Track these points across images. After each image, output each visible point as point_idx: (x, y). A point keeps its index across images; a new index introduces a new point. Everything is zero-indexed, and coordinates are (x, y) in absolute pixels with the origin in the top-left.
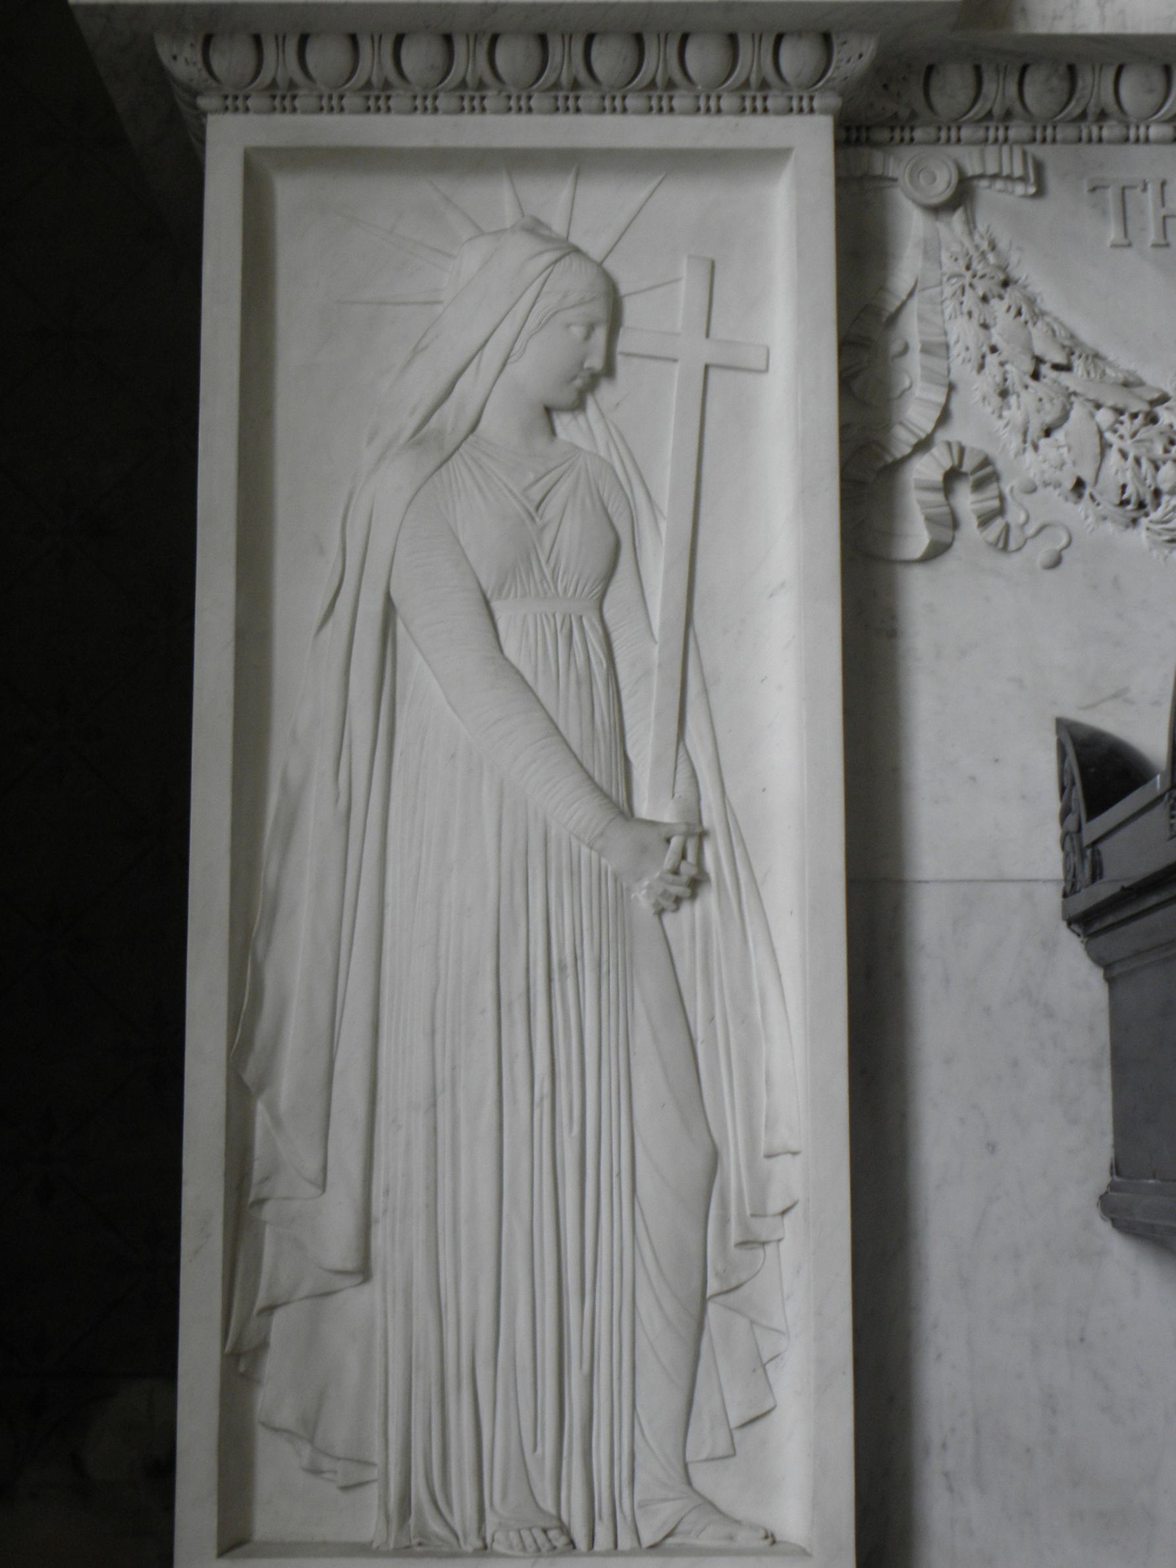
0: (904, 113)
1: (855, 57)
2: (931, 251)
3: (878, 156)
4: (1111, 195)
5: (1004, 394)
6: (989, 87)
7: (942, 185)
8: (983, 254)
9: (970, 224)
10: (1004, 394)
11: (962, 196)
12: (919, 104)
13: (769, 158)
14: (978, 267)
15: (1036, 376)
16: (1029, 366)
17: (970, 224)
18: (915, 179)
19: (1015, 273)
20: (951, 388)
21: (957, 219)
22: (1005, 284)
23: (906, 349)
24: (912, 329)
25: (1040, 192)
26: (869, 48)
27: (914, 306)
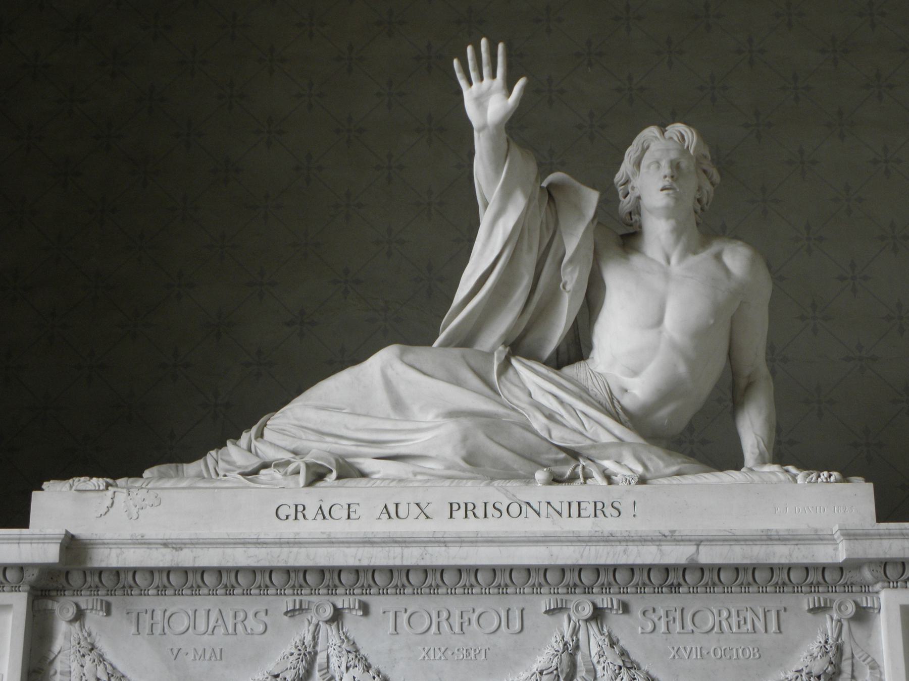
0: (60, 587)
1: (31, 576)
2: (67, 637)
3: (50, 603)
4: (134, 615)
6: (89, 579)
7: (71, 612)
8: (86, 638)
9: (82, 627)
11: (80, 616)
12: (65, 584)
14: (82, 643)
17: (82, 627)
19: (97, 644)
21: (77, 624)
22: (92, 649)
23: (56, 673)
24: (58, 666)
25: (108, 613)
26: (36, 572)
27: (60, 657)
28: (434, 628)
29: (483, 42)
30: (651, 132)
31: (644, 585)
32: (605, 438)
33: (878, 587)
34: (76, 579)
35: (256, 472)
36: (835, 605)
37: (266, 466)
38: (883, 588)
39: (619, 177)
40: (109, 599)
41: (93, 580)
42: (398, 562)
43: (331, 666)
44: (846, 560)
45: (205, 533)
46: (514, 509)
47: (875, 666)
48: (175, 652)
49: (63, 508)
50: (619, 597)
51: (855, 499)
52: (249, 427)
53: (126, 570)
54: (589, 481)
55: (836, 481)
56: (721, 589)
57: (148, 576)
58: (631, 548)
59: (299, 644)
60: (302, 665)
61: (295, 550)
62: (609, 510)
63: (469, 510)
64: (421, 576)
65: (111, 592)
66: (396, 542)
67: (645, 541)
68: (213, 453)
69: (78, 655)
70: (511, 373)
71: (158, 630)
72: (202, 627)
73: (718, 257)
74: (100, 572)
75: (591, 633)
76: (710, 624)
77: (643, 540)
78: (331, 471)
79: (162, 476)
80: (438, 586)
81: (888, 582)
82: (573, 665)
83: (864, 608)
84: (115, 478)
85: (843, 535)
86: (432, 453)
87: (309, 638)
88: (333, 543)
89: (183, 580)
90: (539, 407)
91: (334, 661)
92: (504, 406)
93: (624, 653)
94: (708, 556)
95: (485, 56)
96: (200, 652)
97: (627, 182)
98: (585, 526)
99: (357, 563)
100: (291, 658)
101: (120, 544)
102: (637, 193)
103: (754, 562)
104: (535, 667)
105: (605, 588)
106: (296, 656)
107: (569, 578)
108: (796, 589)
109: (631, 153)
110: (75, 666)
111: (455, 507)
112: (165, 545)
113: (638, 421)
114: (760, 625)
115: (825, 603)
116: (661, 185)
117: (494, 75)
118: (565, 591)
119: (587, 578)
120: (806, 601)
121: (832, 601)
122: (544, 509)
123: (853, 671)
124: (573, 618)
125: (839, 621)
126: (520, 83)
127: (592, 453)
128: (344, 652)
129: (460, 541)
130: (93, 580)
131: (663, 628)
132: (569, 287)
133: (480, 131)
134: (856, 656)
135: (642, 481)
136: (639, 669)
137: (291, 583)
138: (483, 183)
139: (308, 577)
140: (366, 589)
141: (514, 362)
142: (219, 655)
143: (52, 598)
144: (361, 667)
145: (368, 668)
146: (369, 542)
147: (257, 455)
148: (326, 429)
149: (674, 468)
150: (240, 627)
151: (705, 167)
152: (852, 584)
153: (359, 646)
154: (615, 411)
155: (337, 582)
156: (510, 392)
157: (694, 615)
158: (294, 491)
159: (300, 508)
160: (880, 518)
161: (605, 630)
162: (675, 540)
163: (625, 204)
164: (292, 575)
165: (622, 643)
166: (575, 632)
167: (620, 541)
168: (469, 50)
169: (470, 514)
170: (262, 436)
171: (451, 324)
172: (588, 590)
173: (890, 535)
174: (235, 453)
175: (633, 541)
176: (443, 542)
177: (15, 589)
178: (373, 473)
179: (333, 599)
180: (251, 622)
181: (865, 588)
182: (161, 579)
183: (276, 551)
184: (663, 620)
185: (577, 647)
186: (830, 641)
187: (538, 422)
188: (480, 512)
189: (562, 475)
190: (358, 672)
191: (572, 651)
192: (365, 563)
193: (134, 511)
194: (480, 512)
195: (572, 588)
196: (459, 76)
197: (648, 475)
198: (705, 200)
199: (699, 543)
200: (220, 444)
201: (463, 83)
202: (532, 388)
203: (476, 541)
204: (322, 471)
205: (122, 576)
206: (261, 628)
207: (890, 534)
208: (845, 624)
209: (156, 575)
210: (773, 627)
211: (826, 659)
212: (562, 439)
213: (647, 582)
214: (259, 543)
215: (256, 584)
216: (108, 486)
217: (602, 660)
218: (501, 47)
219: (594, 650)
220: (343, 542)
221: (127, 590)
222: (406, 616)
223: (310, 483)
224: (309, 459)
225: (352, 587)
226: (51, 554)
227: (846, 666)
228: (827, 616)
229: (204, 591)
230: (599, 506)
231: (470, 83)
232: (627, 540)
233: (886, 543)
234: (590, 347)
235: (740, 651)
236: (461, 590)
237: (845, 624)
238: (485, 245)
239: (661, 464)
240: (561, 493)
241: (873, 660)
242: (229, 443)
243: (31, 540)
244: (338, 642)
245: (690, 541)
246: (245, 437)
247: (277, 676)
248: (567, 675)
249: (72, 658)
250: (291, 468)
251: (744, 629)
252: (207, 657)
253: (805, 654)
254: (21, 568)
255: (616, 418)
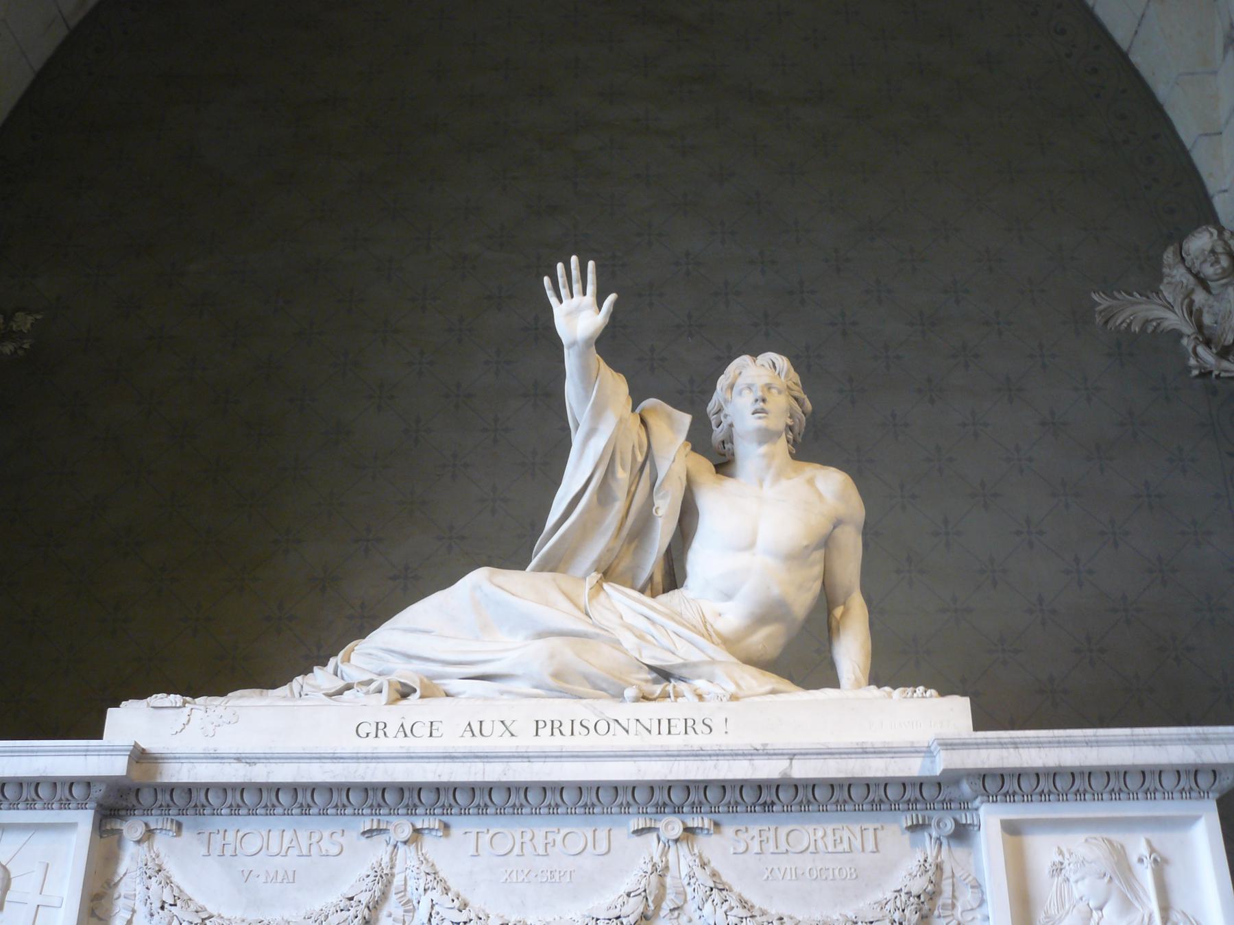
1: (98, 792)
5: (152, 915)
6: (159, 797)
9: (150, 848)
10: (152, 915)
12: (135, 803)
13: (72, 826)
14: (150, 865)
15: (162, 908)
16: (159, 905)
17: (150, 848)
18: (132, 829)
19: (164, 866)
20: (134, 911)
24: (123, 889)
26: (103, 788)
28: (517, 850)
29: (574, 259)
30: (745, 359)
31: (737, 804)
32: (695, 656)
33: (977, 803)
34: (146, 798)
35: (340, 692)
36: (934, 823)
37: (349, 687)
38: (982, 802)
39: (711, 407)
40: (180, 818)
41: (164, 798)
42: (479, 778)
43: (409, 889)
44: (945, 771)
45: (280, 747)
46: (602, 727)
47: (977, 886)
48: (246, 874)
49: (135, 724)
50: (710, 816)
51: (954, 714)
52: (336, 655)
53: (199, 786)
54: (680, 700)
55: (931, 696)
56: (816, 808)
57: (221, 794)
58: (721, 762)
59: (376, 865)
60: (378, 888)
61: (372, 765)
62: (700, 727)
63: (555, 728)
64: (505, 795)
65: (182, 812)
66: (477, 757)
67: (737, 755)
68: (299, 679)
69: (145, 877)
70: (602, 596)
71: (229, 850)
72: (274, 848)
73: (811, 482)
74: (171, 789)
75: (681, 854)
76: (805, 844)
77: (735, 755)
78: (415, 691)
79: (242, 697)
80: (522, 806)
81: (990, 797)
82: (662, 886)
83: (964, 825)
84: (194, 696)
85: (940, 745)
86: (519, 672)
87: (386, 859)
88: (412, 758)
89: (256, 799)
90: (630, 628)
91: (412, 884)
92: (594, 625)
93: (714, 874)
94: (803, 770)
95: (575, 273)
96: (272, 875)
97: (719, 411)
98: (677, 741)
99: (436, 779)
100: (368, 880)
101: (192, 758)
102: (729, 420)
103: (850, 775)
104: (624, 888)
105: (696, 808)
106: (371, 878)
107: (659, 797)
108: (894, 806)
109: (722, 382)
110: (140, 889)
111: (541, 724)
112: (238, 759)
113: (728, 643)
114: (857, 843)
115: (924, 819)
116: (753, 409)
117: (584, 294)
118: (654, 810)
119: (677, 797)
120: (906, 820)
121: (930, 818)
122: (633, 726)
123: (953, 891)
124: (662, 838)
125: (938, 839)
126: (612, 298)
127: (684, 672)
128: (423, 874)
129: (545, 756)
130: (164, 798)
131: (755, 847)
132: (661, 513)
133: (569, 348)
134: (957, 875)
135: (734, 698)
136: (731, 891)
137: (369, 802)
138: (574, 406)
139: (386, 796)
140: (447, 809)
141: (605, 586)
142: (291, 878)
143: (122, 818)
144: (439, 888)
145: (447, 890)
146: (450, 757)
147: (343, 678)
148: (412, 652)
149: (768, 688)
150: (314, 849)
151: (796, 394)
152: (951, 801)
153: (438, 868)
154: (707, 632)
155: (416, 800)
156: (601, 613)
157: (788, 835)
158: (375, 707)
159: (381, 726)
160: (977, 727)
161: (696, 851)
162: (767, 754)
163: (718, 434)
164: (371, 793)
165: (713, 864)
166: (665, 853)
167: (710, 755)
168: (560, 266)
169: (556, 731)
170: (349, 660)
171: (543, 549)
172: (678, 810)
173: (988, 745)
174: (321, 678)
175: (724, 755)
176: (526, 757)
177: (82, 806)
178: (459, 694)
179: (413, 819)
180: (325, 844)
181: (965, 804)
182: (234, 797)
183: (353, 766)
184: (757, 840)
185: (667, 868)
186: (929, 860)
187: (629, 641)
188: (566, 729)
189: (652, 694)
190: (435, 895)
191: (661, 872)
192: (445, 779)
193: (211, 727)
194: (566, 729)
195: (661, 809)
196: (550, 294)
197: (741, 694)
198: (796, 429)
199: (792, 756)
200: (307, 670)
201: (553, 300)
202: (622, 609)
203: (560, 756)
204: (406, 690)
205: (194, 794)
206: (336, 850)
207: (987, 743)
208: (945, 842)
209: (229, 793)
210: (870, 846)
211: (926, 878)
212: (653, 658)
213: (739, 800)
214: (335, 758)
215: (333, 803)
216: (185, 703)
217: (693, 881)
218: (591, 264)
219: (684, 870)
220: (422, 758)
221: (199, 810)
222: (488, 837)
223: (392, 702)
224: (394, 678)
225: (433, 806)
226: (117, 767)
227: (946, 887)
228: (926, 834)
229: (279, 810)
230: (690, 723)
231: (561, 301)
232: (718, 754)
233: (984, 753)
234: (684, 577)
235: (837, 872)
236: (546, 810)
237: (945, 842)
238: (576, 467)
239: (754, 683)
240: (649, 711)
241: (975, 879)
242: (316, 669)
243: (98, 752)
244: (417, 864)
245: (782, 754)
246: (332, 661)
247: (351, 899)
248: (656, 897)
249: (138, 880)
250: (373, 686)
251: (840, 848)
252: (279, 879)
253: (904, 873)
254: (88, 783)
255: (709, 637)
